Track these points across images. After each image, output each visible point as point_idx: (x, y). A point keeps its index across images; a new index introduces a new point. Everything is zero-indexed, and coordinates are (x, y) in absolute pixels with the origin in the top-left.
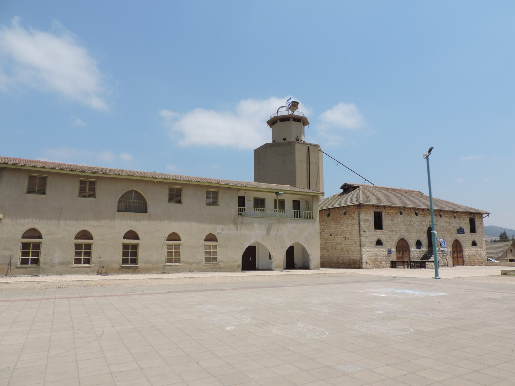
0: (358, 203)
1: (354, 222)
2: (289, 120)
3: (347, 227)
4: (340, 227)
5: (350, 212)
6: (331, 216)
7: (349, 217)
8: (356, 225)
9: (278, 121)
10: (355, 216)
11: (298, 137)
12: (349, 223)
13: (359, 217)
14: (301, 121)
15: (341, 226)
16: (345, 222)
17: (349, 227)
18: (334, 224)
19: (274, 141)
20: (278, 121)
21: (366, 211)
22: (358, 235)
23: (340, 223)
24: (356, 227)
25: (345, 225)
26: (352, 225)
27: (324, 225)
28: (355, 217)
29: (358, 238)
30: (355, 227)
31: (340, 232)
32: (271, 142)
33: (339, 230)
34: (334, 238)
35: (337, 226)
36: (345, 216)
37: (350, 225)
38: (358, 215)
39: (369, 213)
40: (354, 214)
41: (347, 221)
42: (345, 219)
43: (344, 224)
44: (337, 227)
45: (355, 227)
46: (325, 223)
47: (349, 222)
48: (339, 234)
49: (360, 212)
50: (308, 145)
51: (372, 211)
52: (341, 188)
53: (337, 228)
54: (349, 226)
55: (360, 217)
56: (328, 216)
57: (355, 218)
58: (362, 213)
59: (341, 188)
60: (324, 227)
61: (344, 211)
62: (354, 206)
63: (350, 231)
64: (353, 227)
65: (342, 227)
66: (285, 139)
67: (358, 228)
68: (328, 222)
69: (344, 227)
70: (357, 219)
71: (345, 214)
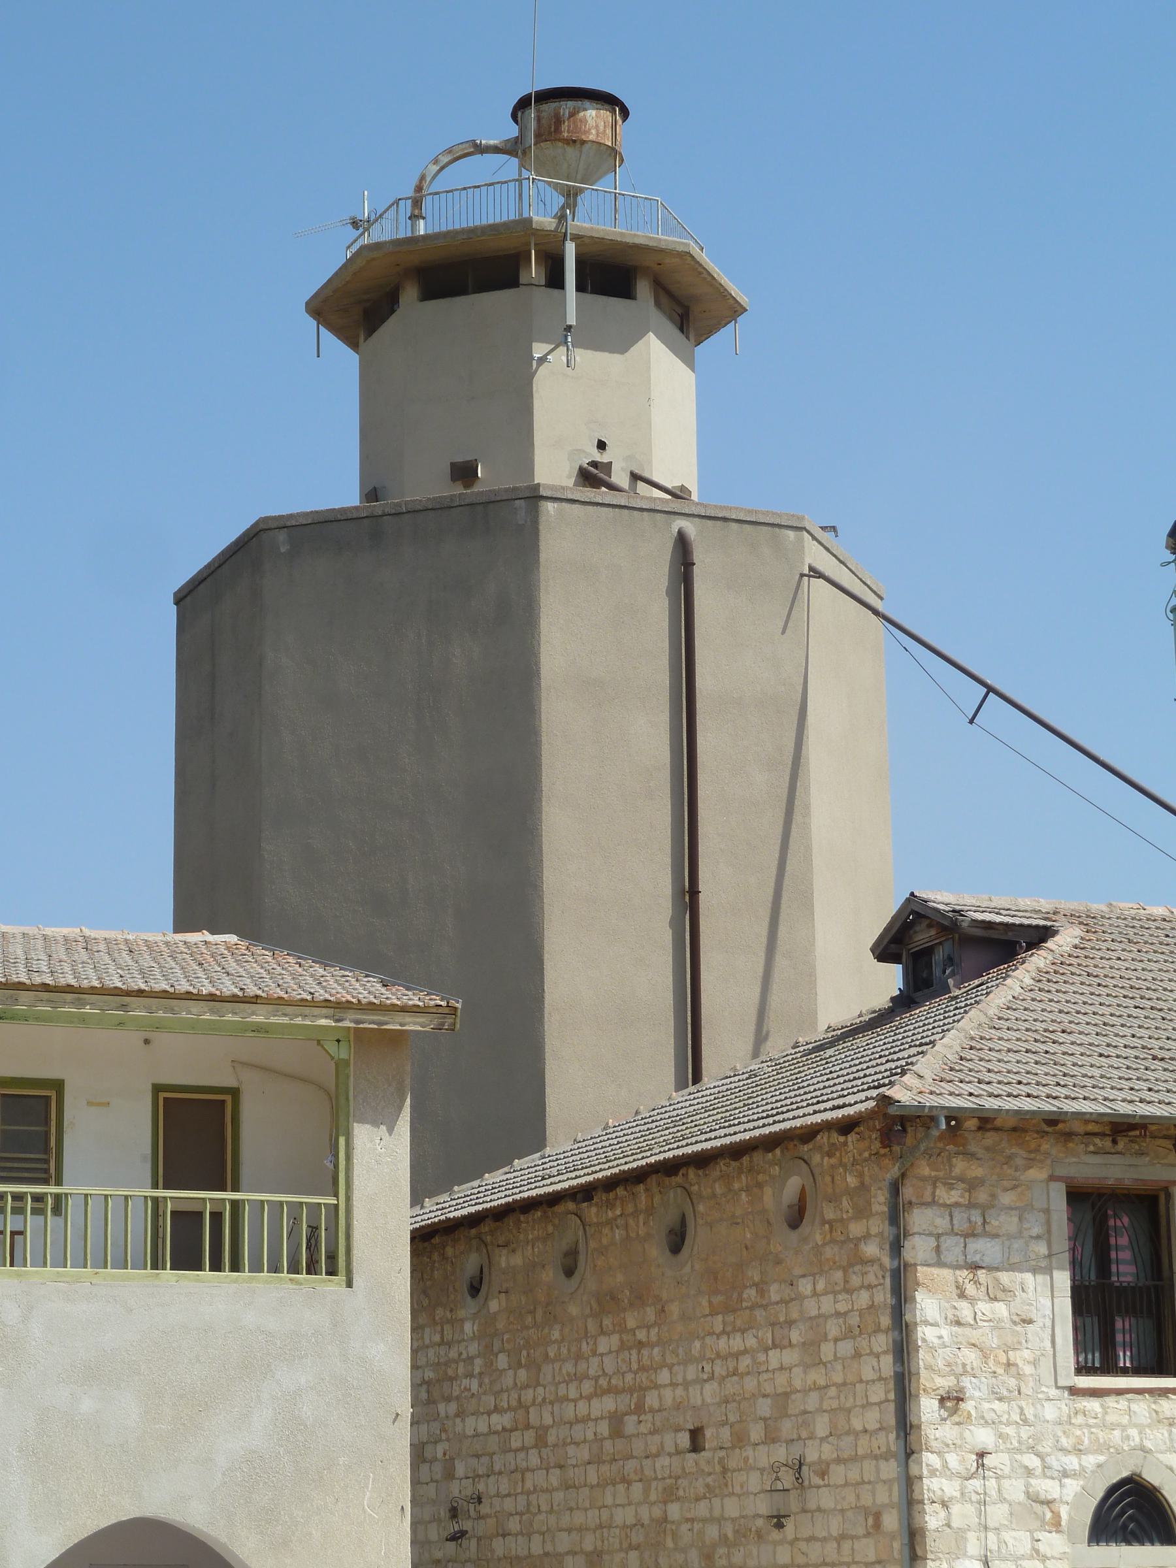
0: (872, 1104)
1: (863, 1299)
2: (512, 282)
3: (811, 1346)
4: (761, 1357)
5: (833, 1199)
6: (699, 1238)
7: (829, 1252)
8: (878, 1330)
9: (410, 294)
10: (867, 1237)
11: (602, 445)
12: (826, 1317)
13: (896, 1248)
14: (643, 288)
15: (766, 1350)
16: (800, 1298)
17: (827, 1350)
18: (718, 1322)
19: (372, 494)
20: (410, 294)
21: (972, 1185)
22: (890, 1440)
23: (759, 1314)
24: (877, 1356)
25: (795, 1336)
26: (848, 1334)
27: (641, 1335)
28: (871, 1249)
29: (890, 1469)
30: (871, 1353)
31: (764, 1407)
32: (357, 503)
33: (750, 1384)
34: (718, 1468)
35: (736, 1343)
36: (794, 1236)
37: (833, 1328)
38: (888, 1230)
39: (1007, 1199)
40: (862, 1213)
41: (815, 1294)
42: (797, 1271)
43: (790, 1323)
44: (737, 1355)
45: (871, 1353)
46: (650, 1313)
47: (827, 1304)
48: (756, 1432)
49: (907, 1192)
50: (680, 523)
51: (1052, 1178)
52: (886, 951)
53: (745, 1362)
54: (825, 1338)
55: (907, 1244)
56: (677, 1240)
57: (871, 1261)
58: (933, 1202)
59: (886, 951)
60: (646, 1361)
61: (793, 1185)
62: (847, 1126)
63: (833, 1391)
64: (857, 1355)
65: (775, 1358)
66: (464, 473)
67: (887, 1364)
68: (674, 1309)
69: (790, 1357)
70: (881, 1266)
71: (797, 1216)
